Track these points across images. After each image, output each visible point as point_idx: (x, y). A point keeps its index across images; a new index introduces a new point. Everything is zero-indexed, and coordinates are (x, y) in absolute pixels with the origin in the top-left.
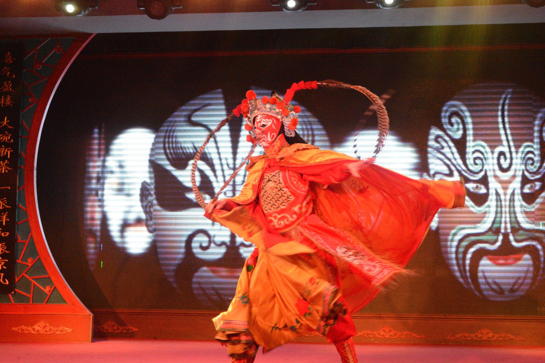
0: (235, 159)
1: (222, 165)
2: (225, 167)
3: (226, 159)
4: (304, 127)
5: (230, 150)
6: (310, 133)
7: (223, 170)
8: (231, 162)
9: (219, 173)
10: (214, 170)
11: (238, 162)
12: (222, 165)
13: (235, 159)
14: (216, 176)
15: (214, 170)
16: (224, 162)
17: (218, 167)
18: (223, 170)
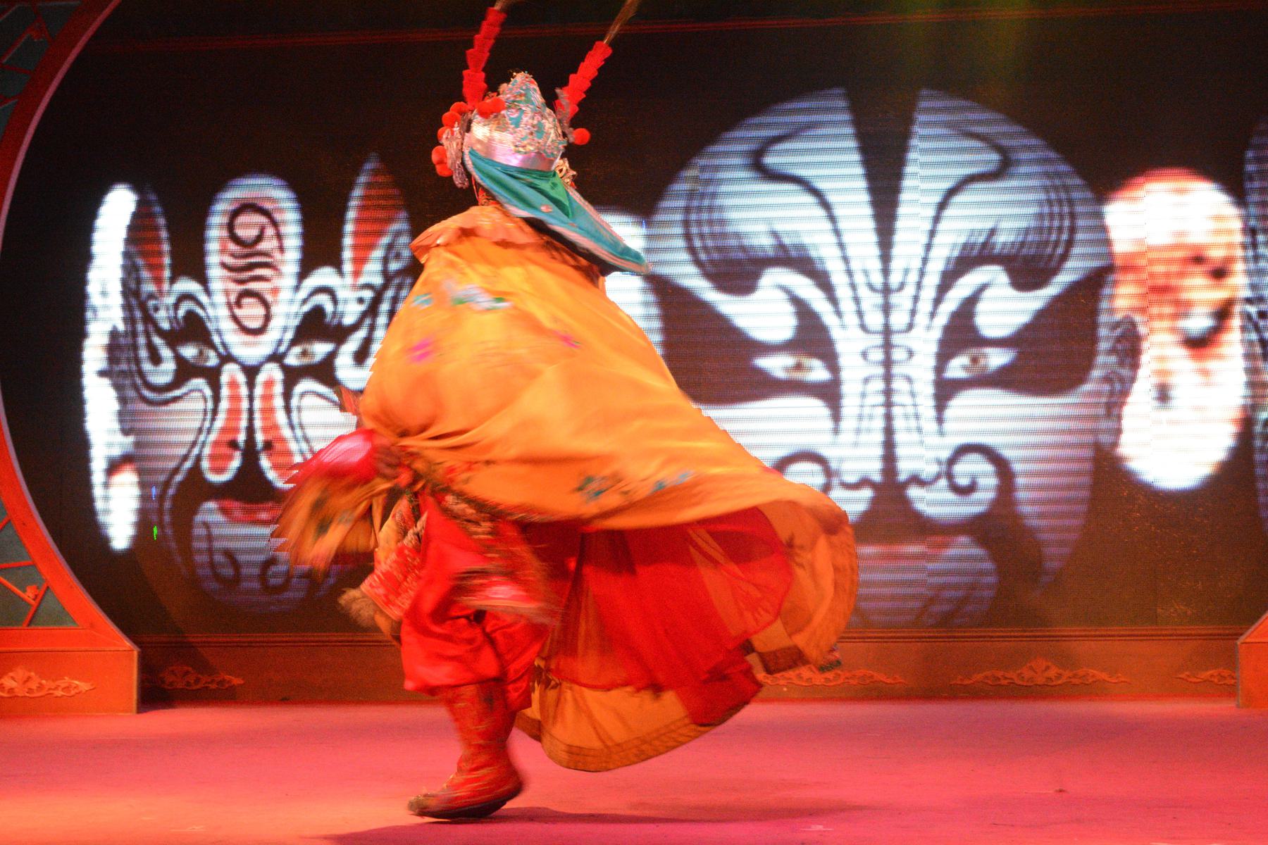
0: (886, 272)
1: (853, 286)
2: (863, 292)
3: (866, 273)
4: (1053, 196)
5: (875, 251)
6: (1066, 209)
7: (857, 300)
8: (877, 280)
9: (847, 305)
10: (833, 300)
11: (895, 280)
12: (853, 286)
13: (886, 272)
14: (839, 313)
15: (833, 300)
16: (859, 279)
17: (843, 292)
18: (857, 300)
